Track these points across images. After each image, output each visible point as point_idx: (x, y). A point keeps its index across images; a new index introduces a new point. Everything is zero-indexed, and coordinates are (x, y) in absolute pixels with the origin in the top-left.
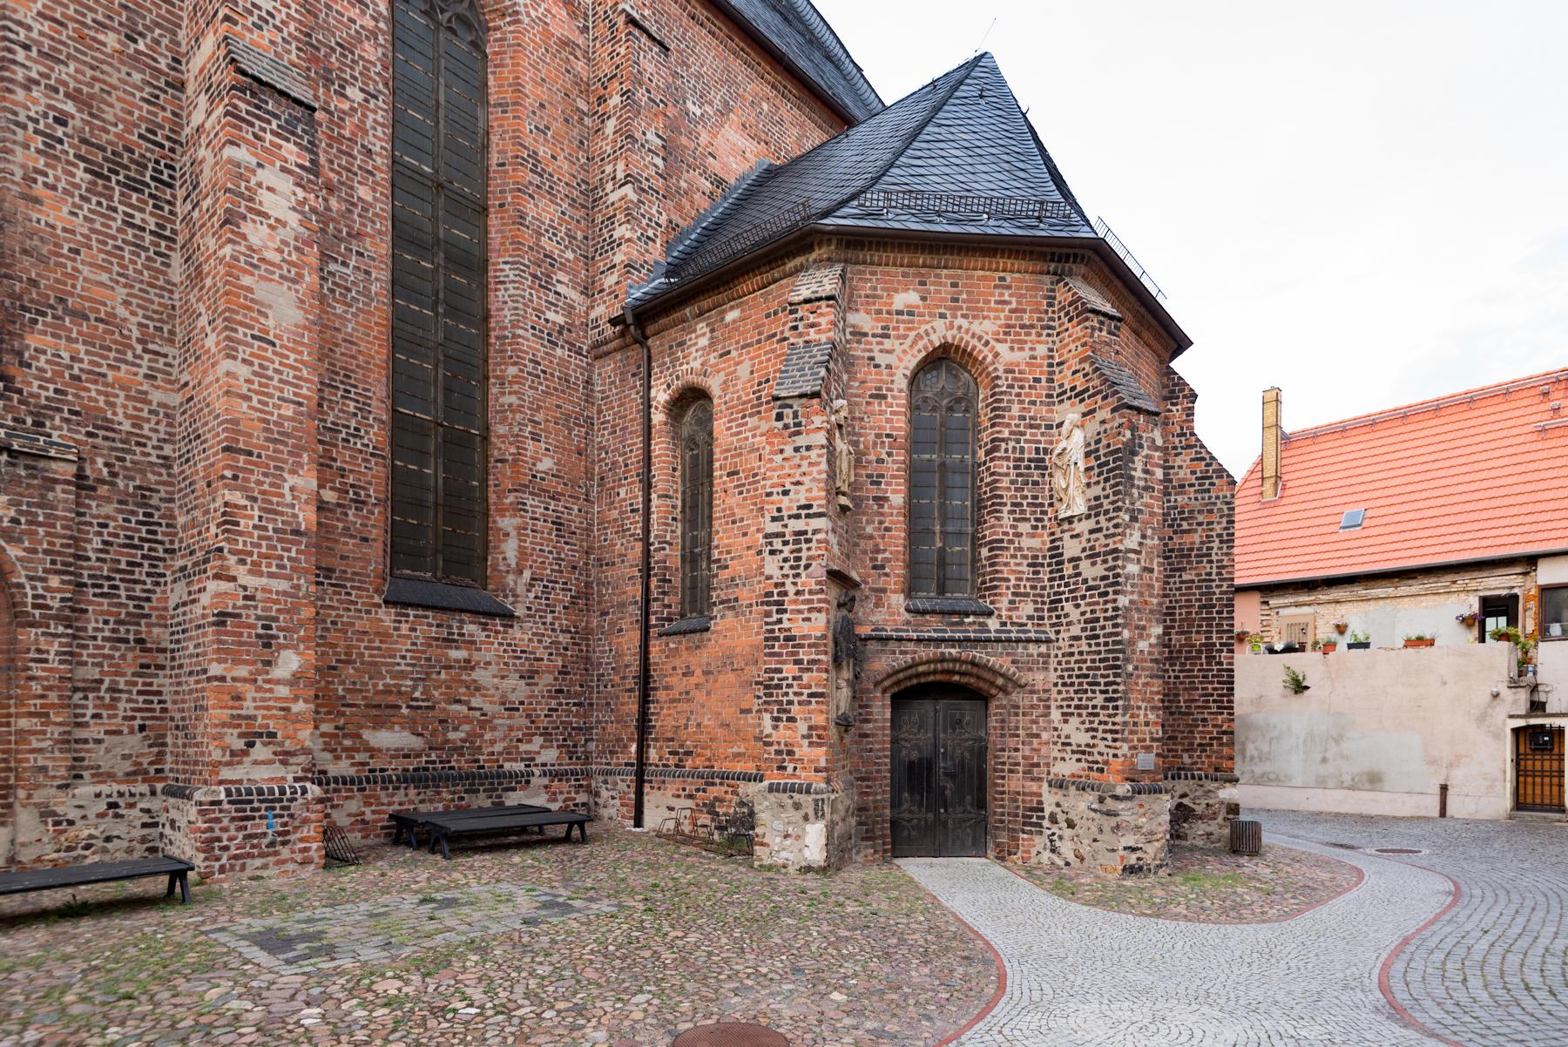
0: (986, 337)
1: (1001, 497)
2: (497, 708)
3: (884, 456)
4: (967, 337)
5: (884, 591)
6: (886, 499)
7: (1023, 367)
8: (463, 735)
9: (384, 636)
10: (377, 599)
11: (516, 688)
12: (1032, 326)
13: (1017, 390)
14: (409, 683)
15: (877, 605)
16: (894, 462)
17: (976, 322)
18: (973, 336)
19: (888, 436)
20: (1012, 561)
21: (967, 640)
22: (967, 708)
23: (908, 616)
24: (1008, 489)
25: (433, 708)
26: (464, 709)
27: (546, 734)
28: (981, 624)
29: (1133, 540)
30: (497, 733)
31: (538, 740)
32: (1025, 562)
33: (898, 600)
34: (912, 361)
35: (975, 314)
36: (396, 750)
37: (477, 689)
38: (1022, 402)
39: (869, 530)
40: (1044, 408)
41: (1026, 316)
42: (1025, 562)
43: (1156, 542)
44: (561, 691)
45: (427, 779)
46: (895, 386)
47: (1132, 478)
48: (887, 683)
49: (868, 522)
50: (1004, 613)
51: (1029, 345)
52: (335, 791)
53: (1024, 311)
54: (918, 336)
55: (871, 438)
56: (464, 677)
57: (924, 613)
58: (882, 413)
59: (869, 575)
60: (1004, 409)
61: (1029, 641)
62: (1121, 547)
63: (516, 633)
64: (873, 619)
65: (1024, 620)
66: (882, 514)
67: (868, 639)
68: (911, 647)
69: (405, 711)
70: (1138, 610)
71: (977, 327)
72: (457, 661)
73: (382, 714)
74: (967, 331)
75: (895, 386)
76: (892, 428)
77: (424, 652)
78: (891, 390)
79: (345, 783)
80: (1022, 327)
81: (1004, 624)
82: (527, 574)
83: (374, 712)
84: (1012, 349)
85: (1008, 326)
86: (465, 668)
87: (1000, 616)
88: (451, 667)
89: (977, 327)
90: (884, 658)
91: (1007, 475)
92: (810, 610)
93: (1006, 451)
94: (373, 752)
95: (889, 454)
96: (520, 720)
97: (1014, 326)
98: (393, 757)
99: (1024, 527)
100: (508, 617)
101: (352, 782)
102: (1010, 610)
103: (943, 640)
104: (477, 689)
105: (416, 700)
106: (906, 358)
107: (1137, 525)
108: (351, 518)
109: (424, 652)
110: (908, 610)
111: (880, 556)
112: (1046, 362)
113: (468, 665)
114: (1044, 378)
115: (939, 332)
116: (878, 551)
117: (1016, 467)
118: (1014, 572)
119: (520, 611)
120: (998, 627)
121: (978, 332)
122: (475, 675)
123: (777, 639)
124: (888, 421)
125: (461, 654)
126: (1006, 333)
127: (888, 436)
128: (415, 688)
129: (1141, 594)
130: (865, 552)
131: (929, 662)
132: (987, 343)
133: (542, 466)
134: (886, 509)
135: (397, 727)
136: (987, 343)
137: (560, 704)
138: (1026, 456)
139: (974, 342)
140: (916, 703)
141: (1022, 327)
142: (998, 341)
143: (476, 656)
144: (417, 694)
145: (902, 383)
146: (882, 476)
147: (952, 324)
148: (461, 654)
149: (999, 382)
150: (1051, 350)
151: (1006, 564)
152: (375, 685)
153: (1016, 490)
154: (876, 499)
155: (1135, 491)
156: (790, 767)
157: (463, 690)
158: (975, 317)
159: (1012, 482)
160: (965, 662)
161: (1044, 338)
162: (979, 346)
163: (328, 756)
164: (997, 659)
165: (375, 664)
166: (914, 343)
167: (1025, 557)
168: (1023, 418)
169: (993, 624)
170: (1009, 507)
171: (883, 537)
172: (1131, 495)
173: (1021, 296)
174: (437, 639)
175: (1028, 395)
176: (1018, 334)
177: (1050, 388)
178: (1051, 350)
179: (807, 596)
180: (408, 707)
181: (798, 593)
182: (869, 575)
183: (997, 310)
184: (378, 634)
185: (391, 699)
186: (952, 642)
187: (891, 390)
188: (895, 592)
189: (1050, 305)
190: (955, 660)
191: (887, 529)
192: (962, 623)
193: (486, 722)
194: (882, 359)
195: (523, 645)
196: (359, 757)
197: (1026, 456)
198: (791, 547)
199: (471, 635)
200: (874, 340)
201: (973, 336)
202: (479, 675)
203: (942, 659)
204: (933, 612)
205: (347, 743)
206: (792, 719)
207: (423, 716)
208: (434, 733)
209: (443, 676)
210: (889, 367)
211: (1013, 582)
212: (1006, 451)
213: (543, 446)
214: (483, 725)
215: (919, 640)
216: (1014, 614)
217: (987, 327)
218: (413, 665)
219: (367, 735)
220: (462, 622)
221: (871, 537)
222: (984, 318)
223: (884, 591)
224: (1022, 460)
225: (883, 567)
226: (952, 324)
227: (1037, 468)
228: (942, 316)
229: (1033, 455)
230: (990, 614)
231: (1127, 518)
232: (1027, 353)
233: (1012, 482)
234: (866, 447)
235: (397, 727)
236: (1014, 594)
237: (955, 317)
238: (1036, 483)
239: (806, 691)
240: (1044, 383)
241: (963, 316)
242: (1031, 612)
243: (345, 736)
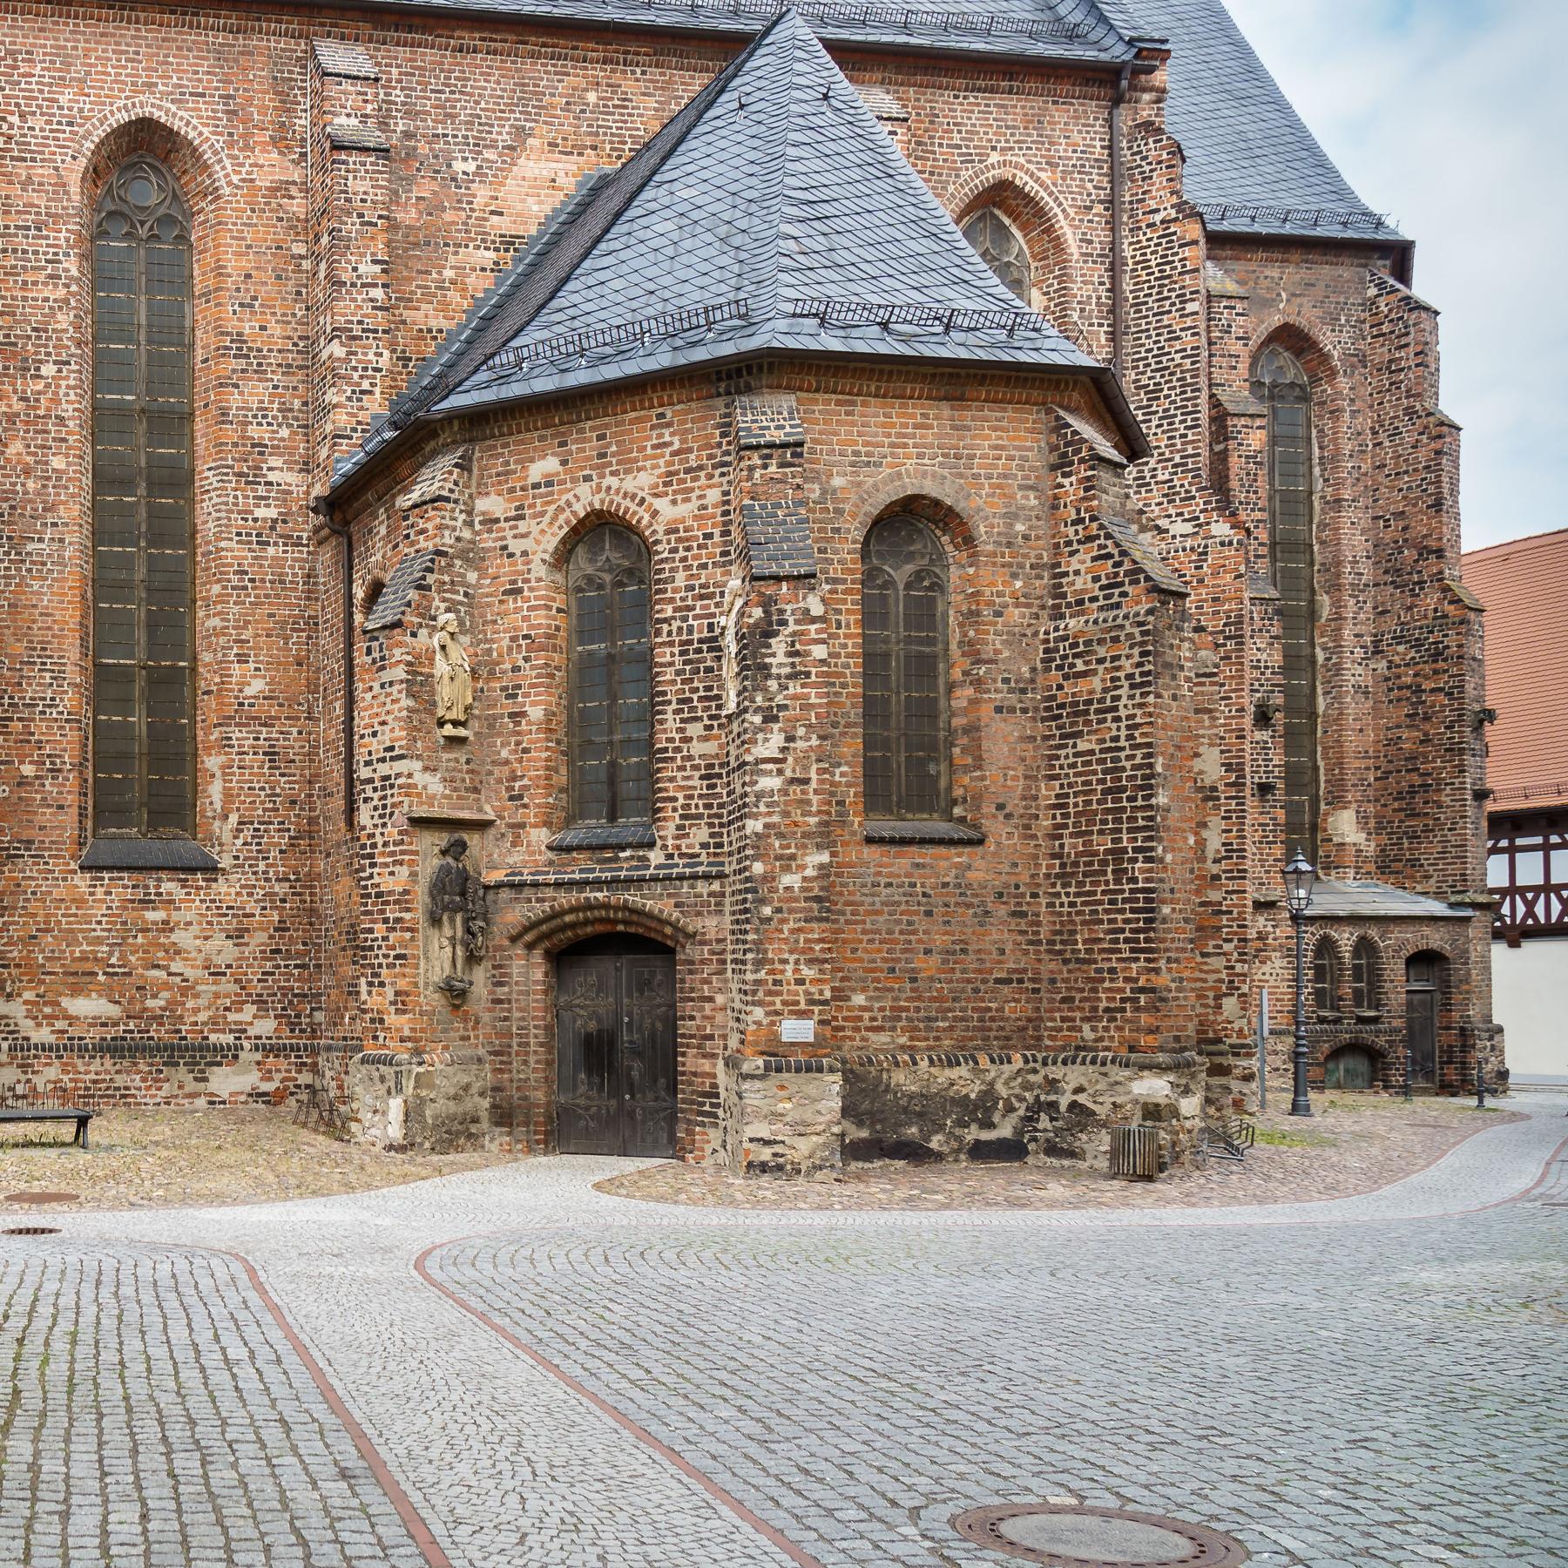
0: (641, 494)
1: (664, 693)
2: (200, 972)
3: (521, 663)
4: (618, 499)
5: (522, 826)
6: (523, 714)
7: (689, 523)
8: (162, 1003)
9: (80, 902)
10: (73, 866)
11: (223, 950)
12: (701, 468)
13: (682, 553)
14: (106, 949)
15: (514, 844)
16: (533, 668)
17: (630, 477)
18: (625, 496)
19: (525, 637)
20: (679, 775)
21: (616, 880)
22: (657, 961)
23: (551, 855)
24: (673, 682)
25: (129, 974)
26: (162, 974)
27: (260, 1002)
28: (640, 859)
29: (771, 744)
30: (200, 1001)
31: (251, 1010)
32: (697, 774)
33: (540, 836)
34: (551, 542)
35: (629, 466)
36: (94, 1018)
37: (178, 952)
38: (689, 568)
39: (504, 754)
40: (719, 571)
41: (692, 456)
42: (697, 774)
43: (814, 742)
44: (278, 951)
45: (123, 1049)
46: (532, 576)
47: (767, 667)
48: (528, 937)
49: (503, 745)
50: (670, 842)
51: (698, 492)
52: (35, 1057)
53: (690, 450)
54: (560, 510)
55: (506, 643)
56: (162, 940)
57: (569, 849)
58: (517, 610)
59: (504, 809)
60: (665, 581)
61: (695, 877)
62: (749, 758)
63: (223, 888)
64: (510, 860)
65: (697, 850)
66: (518, 733)
67: (499, 886)
68: (549, 893)
69: (101, 978)
70: (780, 835)
71: (629, 484)
72: (155, 923)
73: (80, 981)
74: (618, 492)
75: (532, 576)
76: (531, 627)
77: (120, 916)
78: (526, 581)
79: (44, 1050)
80: (687, 471)
81: (670, 856)
82: (234, 819)
83: (71, 979)
84: (674, 502)
85: (670, 474)
86: (164, 930)
87: (665, 847)
88: (148, 930)
89: (629, 484)
90: (518, 906)
91: (671, 664)
92: (395, 863)
93: (670, 634)
94: (72, 1020)
95: (526, 659)
96: (229, 987)
97: (676, 473)
98: (90, 1025)
99: (695, 730)
100: (211, 870)
101: (51, 1050)
102: (677, 837)
103: (586, 882)
104: (178, 952)
105: (113, 966)
106: (544, 540)
107: (776, 727)
108: (48, 788)
109: (120, 916)
110: (550, 848)
111: (517, 785)
112: (719, 511)
113: (167, 927)
114: (717, 532)
115: (584, 499)
116: (514, 778)
117: (682, 653)
118: (682, 788)
119: (226, 862)
120: (662, 860)
121: (631, 490)
122: (174, 937)
123: (369, 896)
124: (525, 619)
125: (159, 915)
126: (666, 484)
127: (525, 637)
128: (111, 954)
129: (786, 814)
130: (499, 781)
131: (573, 910)
132: (643, 501)
133: (249, 691)
134: (524, 727)
135: (94, 995)
136: (643, 501)
137: (278, 967)
138: (696, 636)
139: (627, 503)
140: (593, 959)
141: (687, 471)
142: (656, 495)
143: (175, 916)
144: (113, 960)
145: (539, 570)
146: (519, 687)
147: (599, 486)
148: (159, 915)
149: (659, 548)
150: (726, 493)
151: (672, 779)
152: (72, 952)
153: (684, 682)
154: (512, 715)
155: (773, 685)
156: (381, 1035)
157: (161, 954)
158: (627, 472)
159: (678, 673)
160: (617, 908)
161: (716, 480)
162: (633, 507)
163: (31, 1023)
164: (656, 903)
165: (72, 931)
166: (554, 518)
167: (696, 768)
168: (691, 588)
169: (656, 857)
170: (674, 706)
171: (520, 761)
172: (765, 690)
173: (687, 431)
174: (133, 901)
175: (695, 558)
176: (684, 481)
177: (725, 543)
178: (726, 493)
179: (392, 848)
180: (105, 973)
181: (385, 844)
182: (504, 809)
183: (655, 457)
184: (73, 901)
185: (88, 966)
186: (597, 884)
187: (526, 581)
188: (535, 826)
189: (723, 435)
190: (606, 906)
191: (525, 751)
192: (616, 859)
193: (188, 989)
194: (515, 546)
195: (230, 900)
196: (60, 1025)
197: (696, 636)
198: (380, 793)
199: (170, 894)
200: (507, 525)
201: (625, 496)
202: (180, 937)
203: (589, 906)
204: (579, 848)
205: (48, 1010)
206: (382, 984)
207: (120, 983)
208: (131, 1000)
209: (140, 940)
210: (525, 553)
211: (681, 801)
212: (670, 634)
213: (252, 666)
214: (184, 992)
215: (558, 885)
216: (683, 843)
217: (641, 481)
218: (109, 930)
219: (66, 1002)
220: (159, 880)
221: (507, 762)
222: (639, 470)
223: (522, 826)
224: (690, 642)
225: (521, 797)
226: (599, 486)
227: (710, 650)
228: (587, 479)
229: (705, 634)
230: (651, 845)
231: (757, 719)
232: (695, 504)
233: (678, 673)
234: (501, 655)
235: (94, 995)
236: (682, 817)
237: (602, 476)
238: (709, 670)
239: (392, 953)
240: (717, 539)
241: (613, 474)
242: (706, 839)
243: (45, 1003)
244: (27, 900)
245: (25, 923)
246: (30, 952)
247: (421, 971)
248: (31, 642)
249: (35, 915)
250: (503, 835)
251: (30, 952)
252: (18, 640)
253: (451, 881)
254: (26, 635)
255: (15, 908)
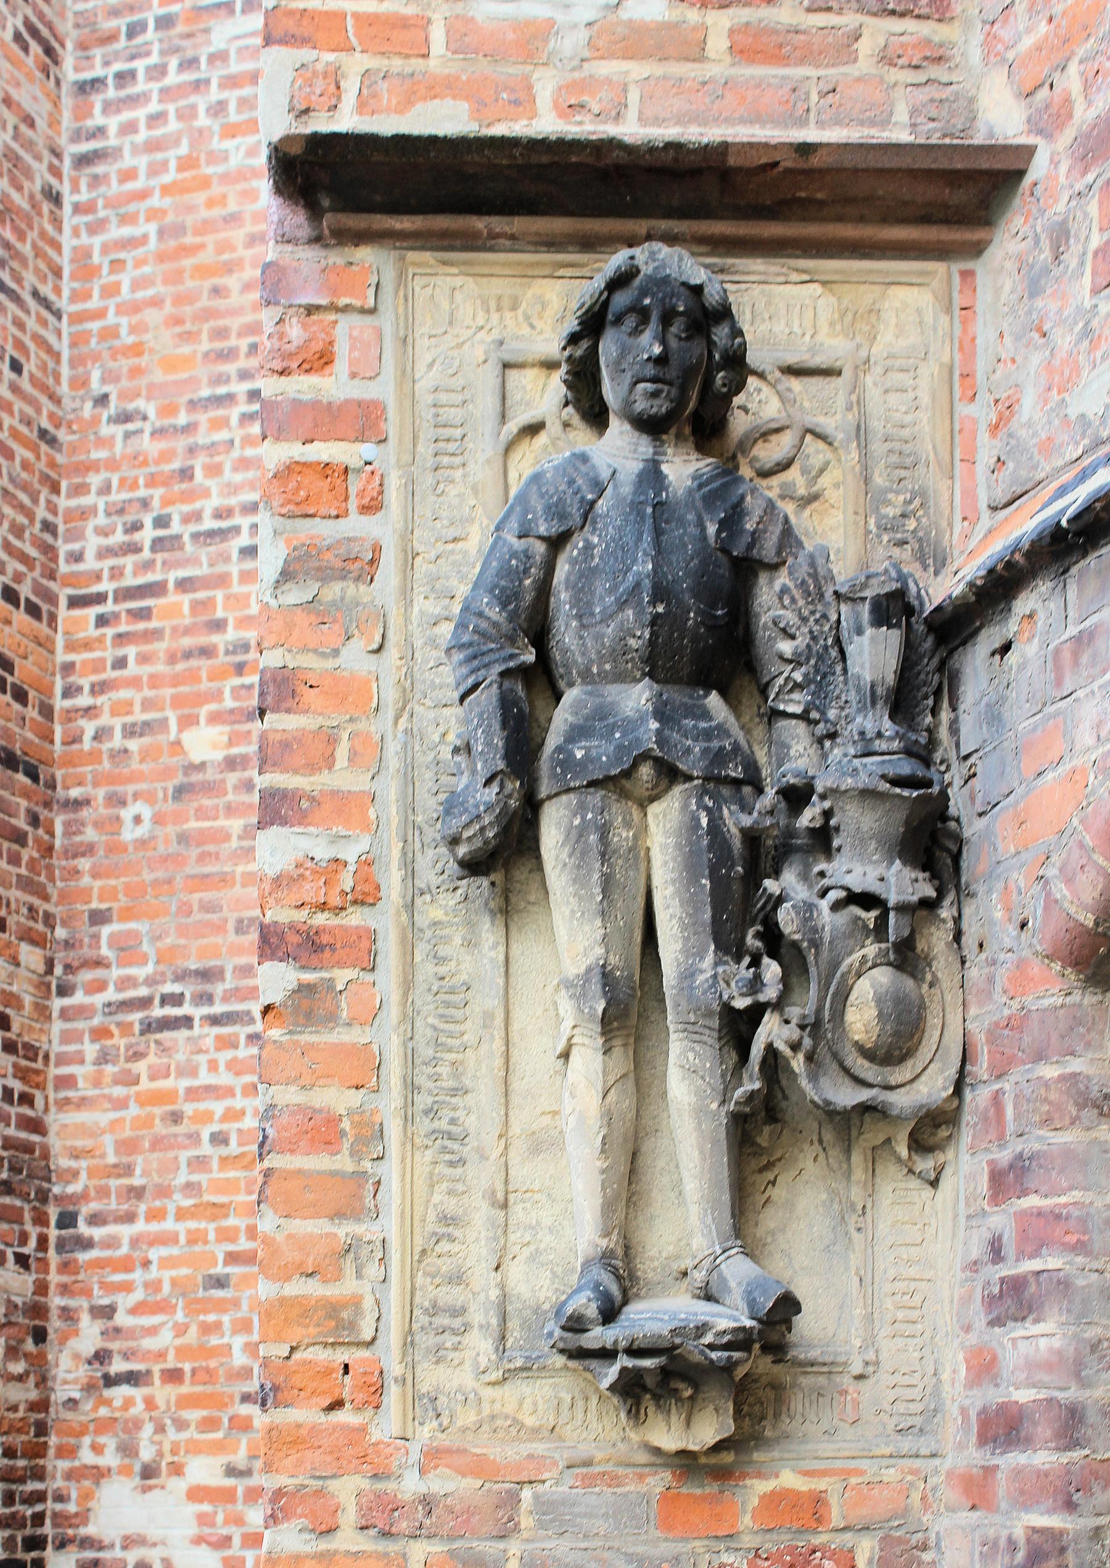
244: (199, 1163)
245: (195, 1238)
246: (207, 1329)
247: (390, 1226)
248: (221, 334)
249: (218, 1211)
250: (1061, 236)
251: (207, 1329)
252: (189, 337)
253: (585, 576)
254: (208, 314)
255: (164, 1192)
